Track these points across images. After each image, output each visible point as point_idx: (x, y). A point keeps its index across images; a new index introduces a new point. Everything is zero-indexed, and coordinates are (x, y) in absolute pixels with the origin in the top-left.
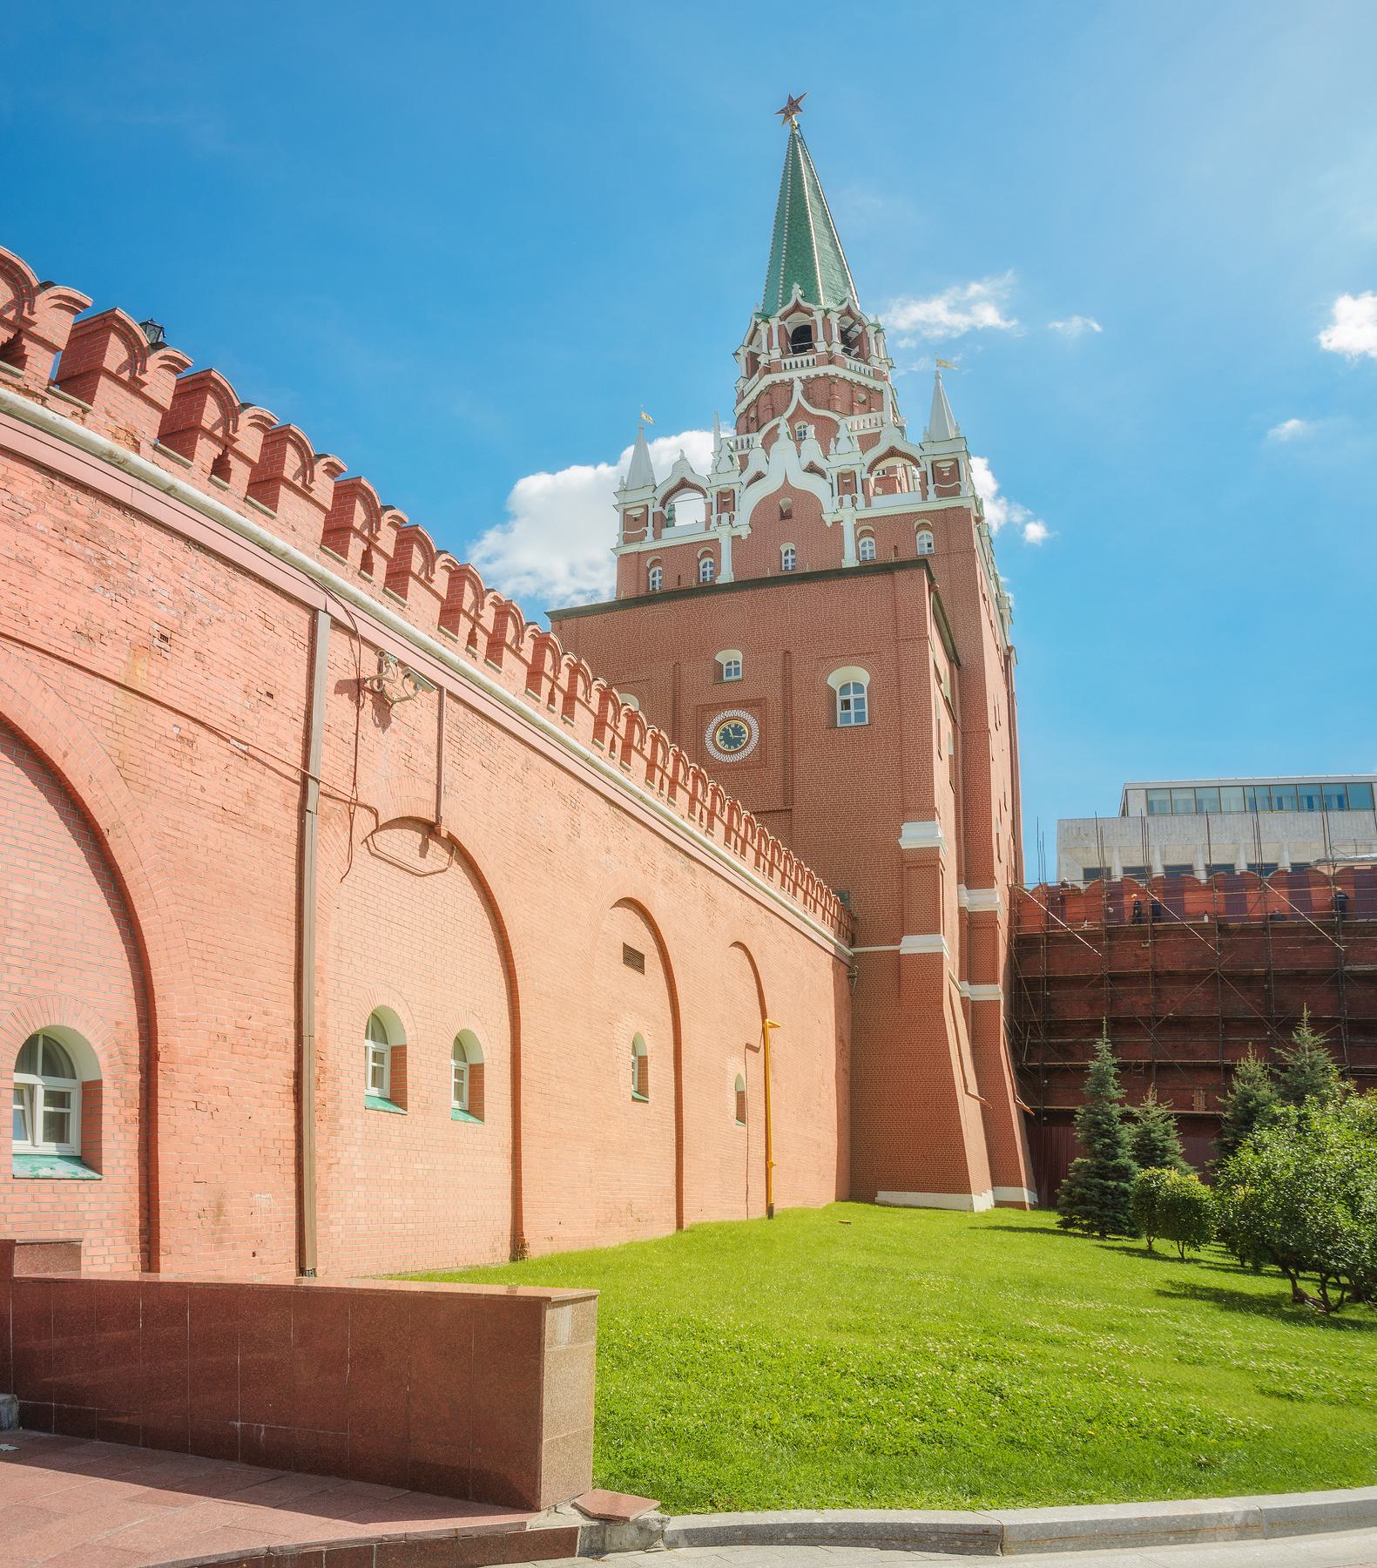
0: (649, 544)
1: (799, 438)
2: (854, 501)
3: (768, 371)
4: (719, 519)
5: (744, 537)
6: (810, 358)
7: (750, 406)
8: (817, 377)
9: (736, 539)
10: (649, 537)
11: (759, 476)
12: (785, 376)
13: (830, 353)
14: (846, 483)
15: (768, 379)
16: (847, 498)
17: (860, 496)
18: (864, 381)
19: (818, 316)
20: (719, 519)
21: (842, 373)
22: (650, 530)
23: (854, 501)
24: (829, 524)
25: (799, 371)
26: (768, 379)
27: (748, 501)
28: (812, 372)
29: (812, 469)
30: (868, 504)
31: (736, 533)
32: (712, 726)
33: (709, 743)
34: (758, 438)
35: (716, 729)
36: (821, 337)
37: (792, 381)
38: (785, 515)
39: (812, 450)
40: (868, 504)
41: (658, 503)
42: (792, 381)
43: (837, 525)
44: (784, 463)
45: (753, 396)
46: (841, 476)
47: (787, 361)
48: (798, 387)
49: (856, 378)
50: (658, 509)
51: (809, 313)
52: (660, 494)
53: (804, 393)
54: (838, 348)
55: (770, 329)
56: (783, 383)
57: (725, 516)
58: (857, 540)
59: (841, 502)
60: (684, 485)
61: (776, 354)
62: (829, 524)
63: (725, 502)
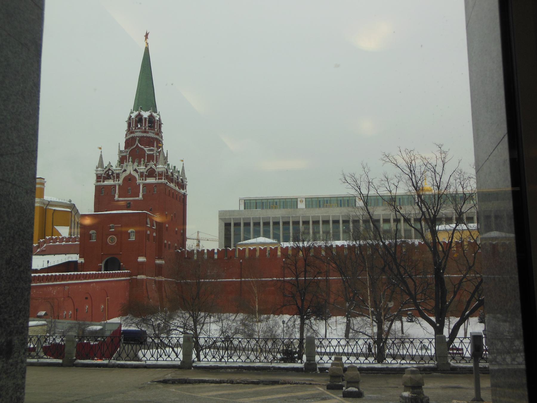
0: (102, 183)
1: (133, 162)
9: (119, 185)
11: (125, 171)
13: (145, 129)
14: (142, 175)
17: (144, 178)
22: (102, 180)
27: (122, 177)
29: (135, 170)
38: (130, 180)
43: (139, 184)
44: (130, 168)
46: (141, 173)
58: (143, 187)
63: (118, 176)
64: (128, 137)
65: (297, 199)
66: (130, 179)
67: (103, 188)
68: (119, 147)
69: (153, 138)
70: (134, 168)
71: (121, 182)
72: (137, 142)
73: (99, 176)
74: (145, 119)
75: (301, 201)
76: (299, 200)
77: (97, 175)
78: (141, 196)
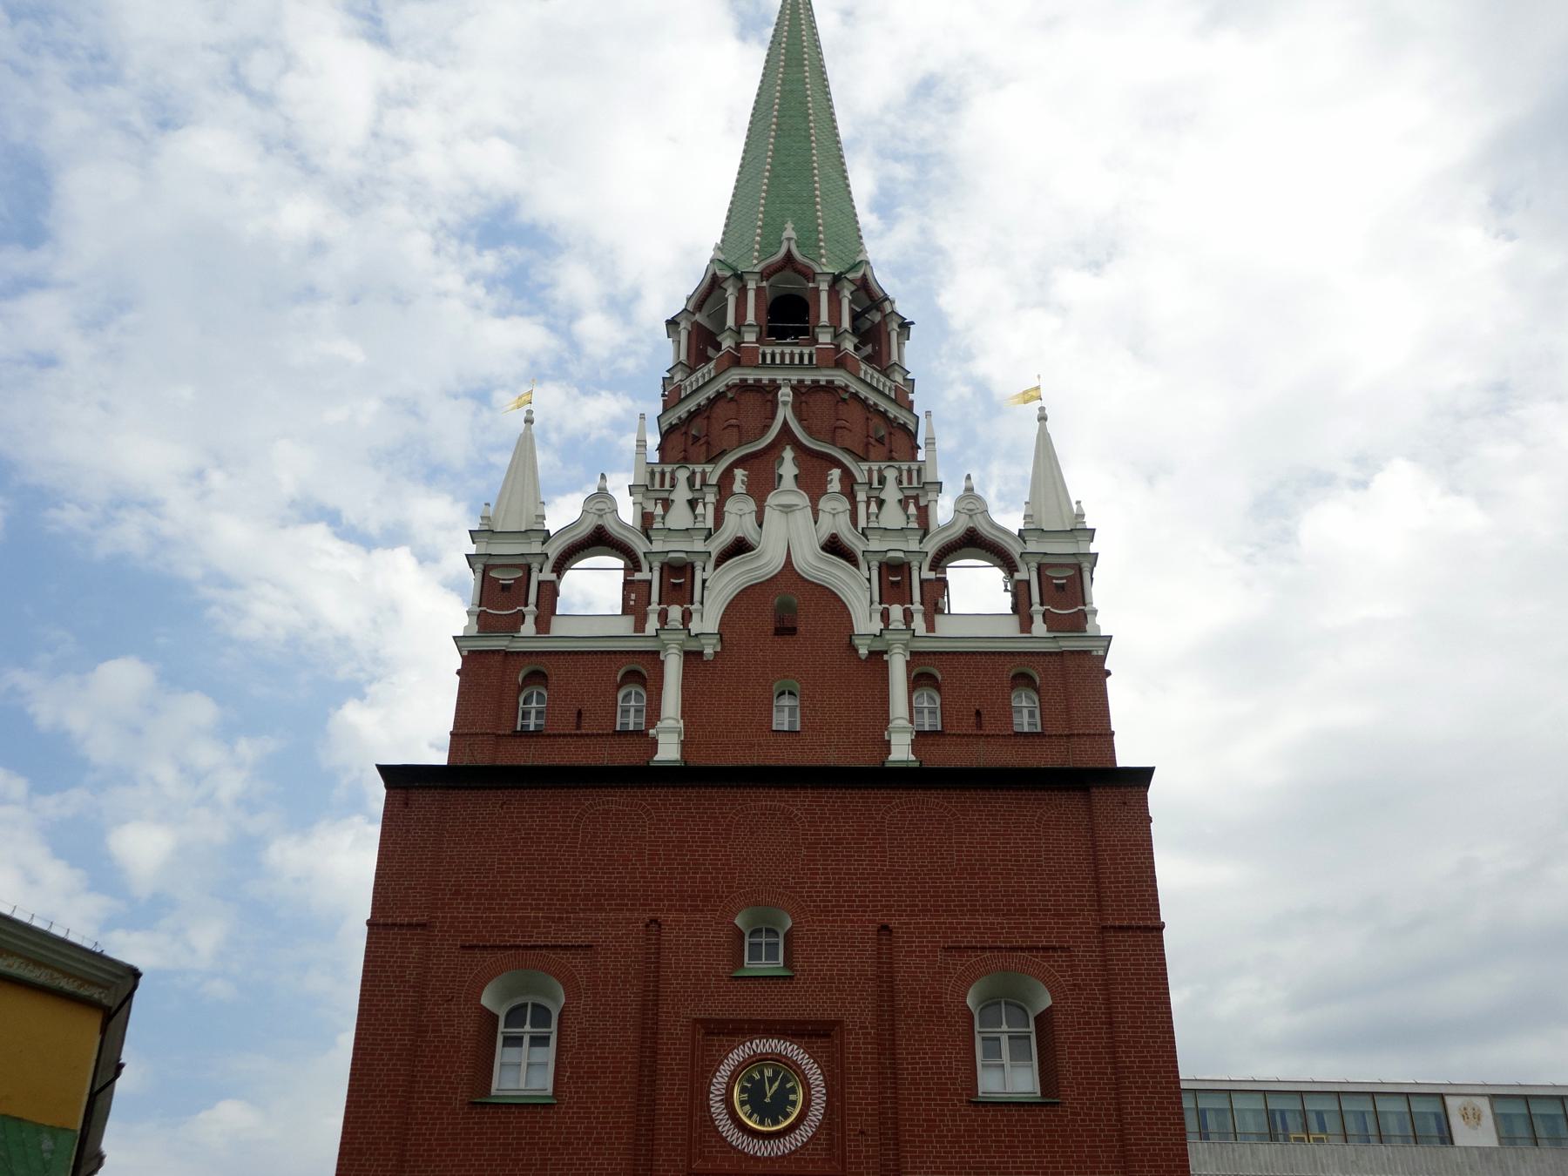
1: (812, 485)
2: (908, 616)
3: (736, 361)
4: (663, 616)
5: (708, 651)
6: (806, 351)
7: (692, 415)
8: (815, 382)
9: (692, 658)
10: (528, 628)
11: (740, 547)
12: (765, 376)
13: (838, 347)
15: (734, 376)
16: (896, 611)
17: (917, 606)
18: (883, 405)
19: (824, 286)
20: (663, 616)
21: (854, 386)
22: (532, 607)
23: (908, 616)
24: (863, 651)
25: (786, 369)
26: (734, 376)
27: (719, 589)
28: (808, 377)
29: (834, 547)
30: (931, 626)
31: (693, 646)
32: (725, 1070)
33: (717, 1107)
34: (714, 473)
35: (733, 1077)
36: (824, 317)
37: (775, 387)
39: (835, 516)
40: (931, 626)
41: (548, 566)
42: (775, 387)
43: (878, 659)
44: (787, 531)
45: (701, 399)
47: (768, 350)
48: (785, 395)
49: (873, 398)
50: (548, 575)
51: (809, 275)
52: (554, 551)
53: (797, 409)
54: (849, 345)
55: (742, 292)
56: (758, 387)
57: (675, 612)
59: (885, 616)
60: (599, 540)
61: (750, 337)
62: (863, 651)
63: (679, 579)
64: (682, 411)
65: (1442, 1096)
66: (786, 614)
67: (537, 677)
68: (642, 444)
69: (884, 414)
70: (824, 534)
71: (707, 620)
72: (784, 413)
73: (505, 588)
74: (836, 280)
75: (1472, 1117)
76: (1453, 1104)
77: (484, 565)
78: (901, 752)
